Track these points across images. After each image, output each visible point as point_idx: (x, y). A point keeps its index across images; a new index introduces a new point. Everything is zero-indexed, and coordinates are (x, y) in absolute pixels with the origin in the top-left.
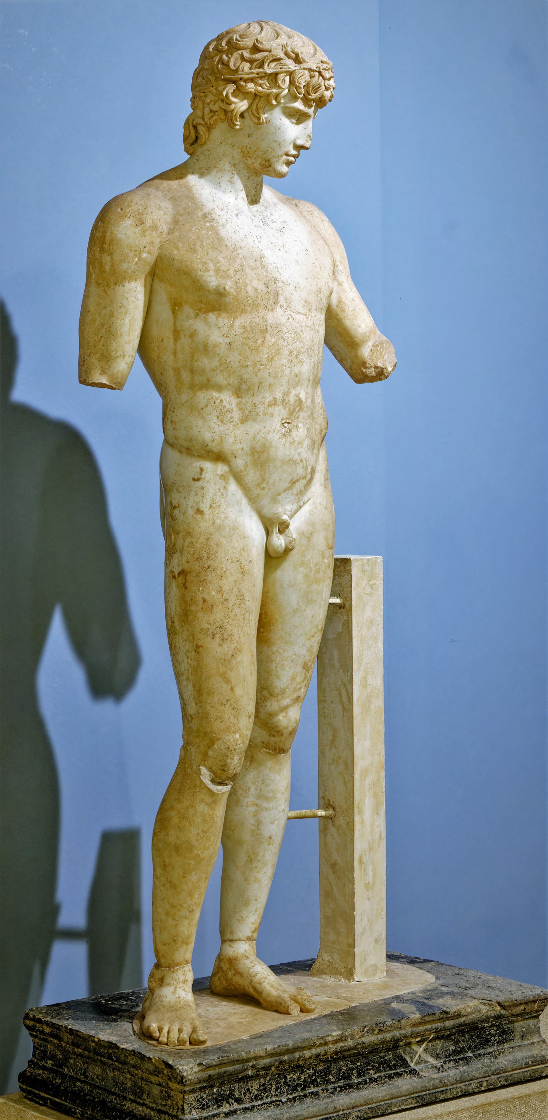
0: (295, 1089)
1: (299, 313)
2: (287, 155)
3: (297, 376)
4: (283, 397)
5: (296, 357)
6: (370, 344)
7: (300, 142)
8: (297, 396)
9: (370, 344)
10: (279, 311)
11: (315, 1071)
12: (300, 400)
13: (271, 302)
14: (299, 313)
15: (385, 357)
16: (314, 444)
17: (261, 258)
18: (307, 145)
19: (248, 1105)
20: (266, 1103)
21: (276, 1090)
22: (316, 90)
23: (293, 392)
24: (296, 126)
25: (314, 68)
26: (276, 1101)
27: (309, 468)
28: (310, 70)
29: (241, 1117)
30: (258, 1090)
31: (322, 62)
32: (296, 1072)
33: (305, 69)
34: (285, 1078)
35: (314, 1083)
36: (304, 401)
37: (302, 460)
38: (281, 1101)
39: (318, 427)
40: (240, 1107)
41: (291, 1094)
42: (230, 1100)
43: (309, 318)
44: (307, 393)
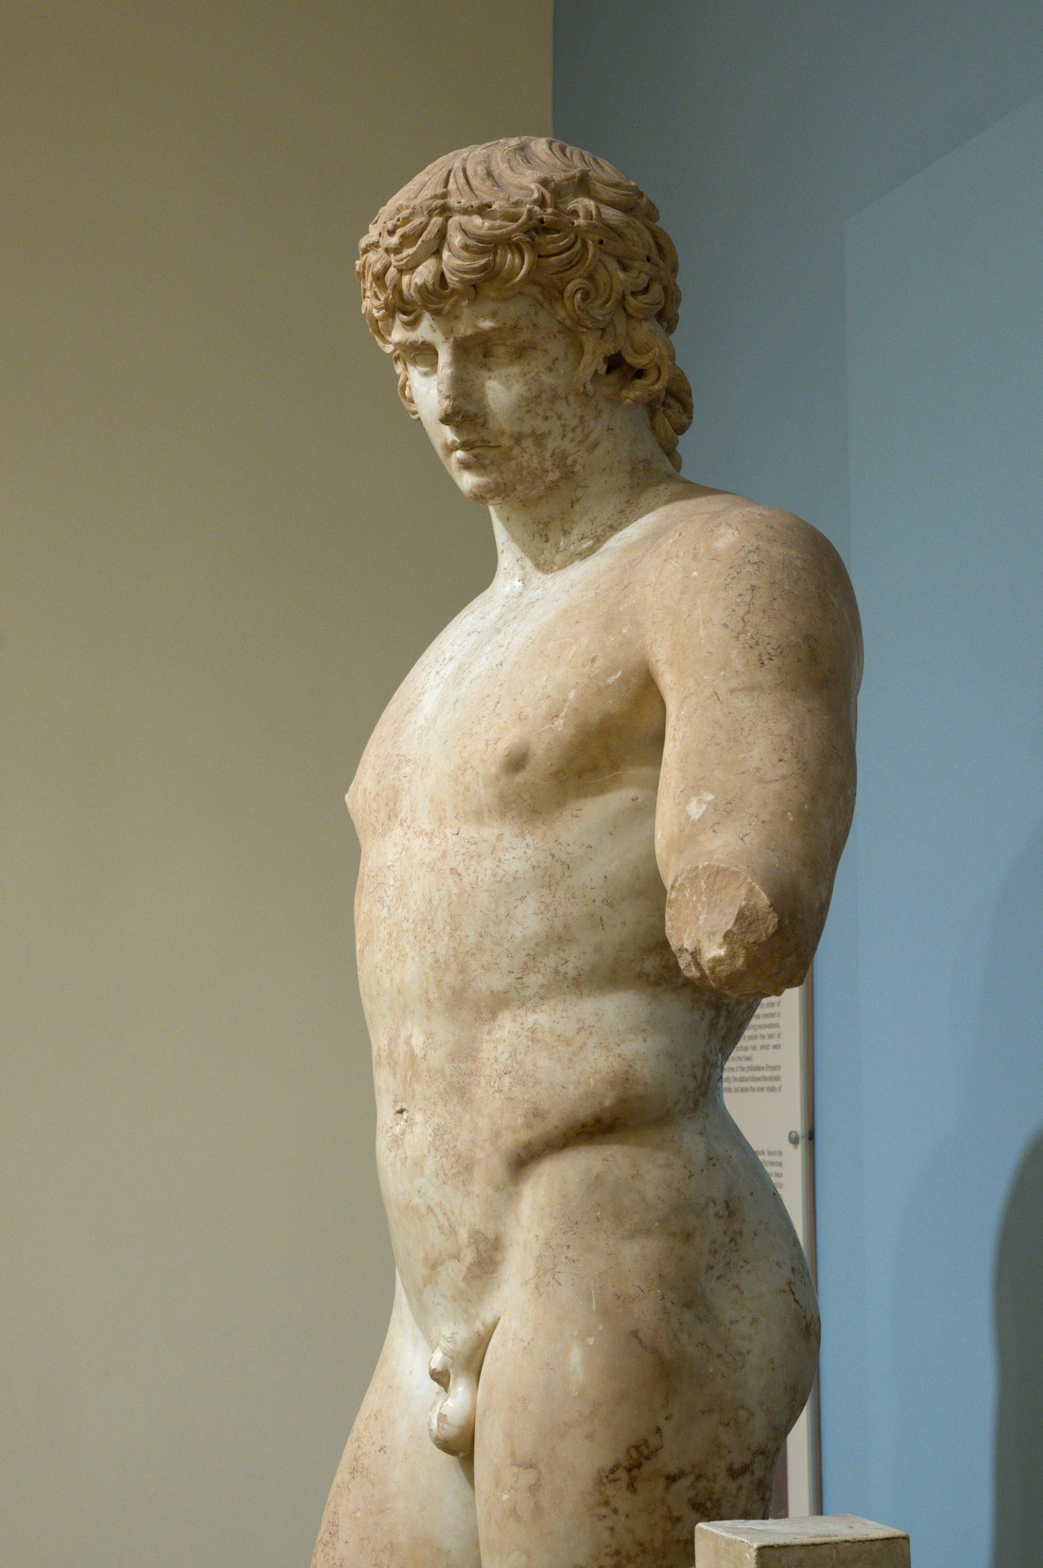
4: (389, 1044)
13: (382, 816)
16: (469, 1169)
27: (463, 1235)
36: (421, 1055)
37: (430, 1209)
39: (483, 1123)
43: (437, 841)
44: (430, 1036)
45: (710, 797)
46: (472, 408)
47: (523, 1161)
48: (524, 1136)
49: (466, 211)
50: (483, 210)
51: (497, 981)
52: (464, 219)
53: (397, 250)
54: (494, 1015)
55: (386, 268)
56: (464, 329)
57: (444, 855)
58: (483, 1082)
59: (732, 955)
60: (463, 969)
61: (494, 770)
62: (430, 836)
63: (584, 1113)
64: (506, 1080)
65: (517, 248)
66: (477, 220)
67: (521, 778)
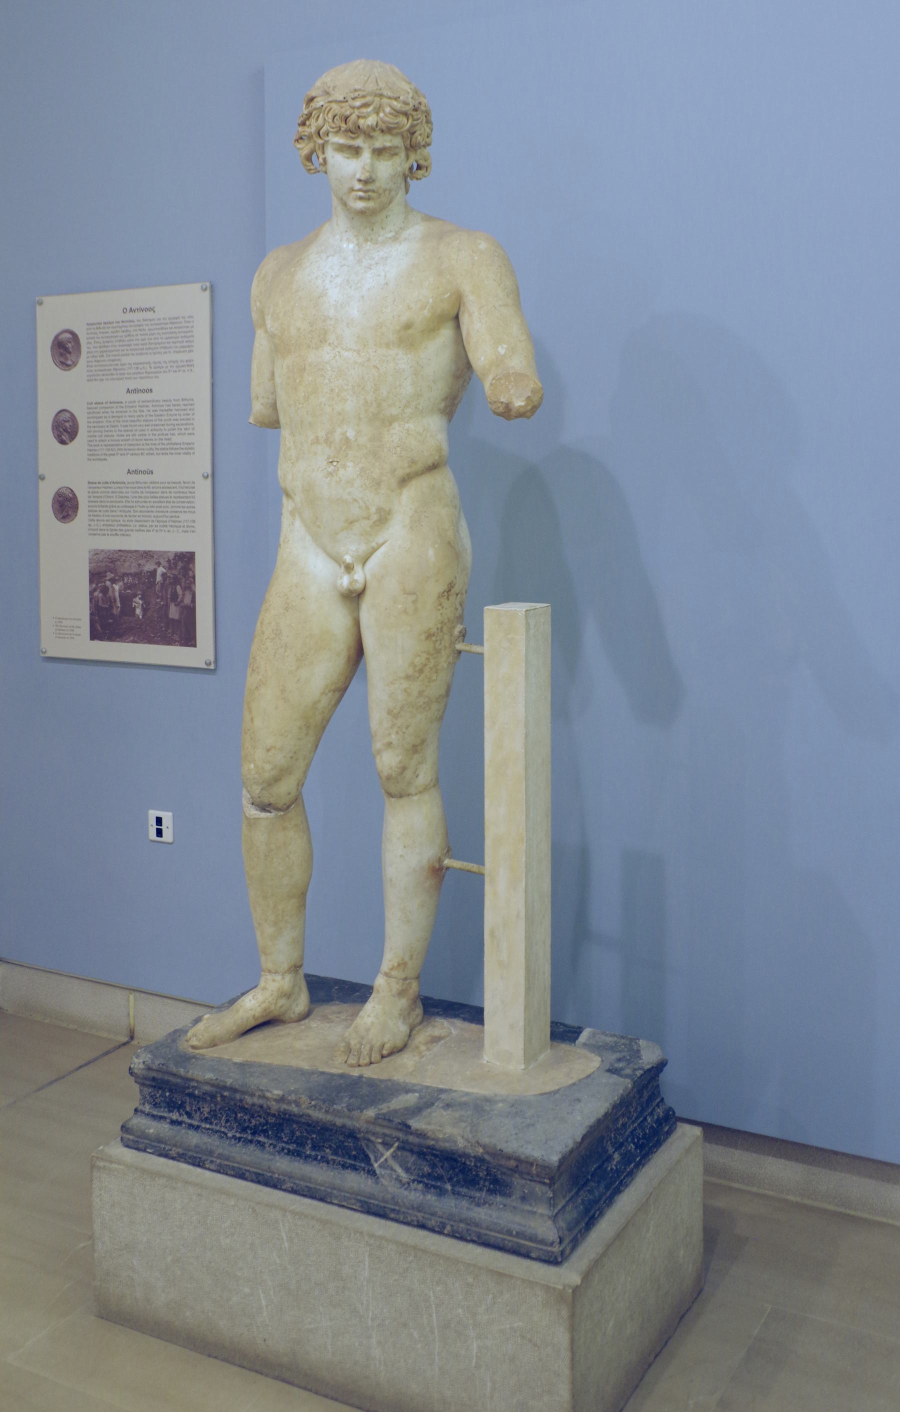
0: (244, 1130)
1: (350, 349)
2: (353, 190)
3: (340, 414)
5: (338, 395)
6: (491, 377)
7: (358, 176)
8: (344, 434)
9: (491, 377)
10: (327, 348)
11: (267, 1121)
12: (347, 440)
14: (350, 349)
15: (512, 391)
17: (319, 297)
18: (363, 178)
19: (196, 1123)
20: (212, 1130)
21: (227, 1121)
22: (346, 119)
23: (339, 431)
24: (355, 160)
25: (341, 98)
26: (223, 1132)
28: (336, 101)
29: (183, 1131)
30: (209, 1113)
31: (356, 90)
32: (246, 1114)
33: (330, 102)
34: (236, 1115)
35: (265, 1132)
38: (226, 1134)
40: (189, 1121)
41: (240, 1133)
42: (181, 1111)
45: (505, 346)
46: (374, 177)
47: (404, 481)
48: (408, 471)
49: (390, 98)
50: (397, 99)
51: (394, 411)
52: (389, 101)
53: (359, 108)
54: (391, 424)
55: (351, 114)
56: (378, 144)
57: (369, 360)
58: (386, 450)
59: (526, 406)
60: (379, 405)
61: (398, 328)
62: (358, 352)
63: (430, 463)
64: (398, 449)
65: (406, 114)
66: (395, 103)
67: (410, 332)
